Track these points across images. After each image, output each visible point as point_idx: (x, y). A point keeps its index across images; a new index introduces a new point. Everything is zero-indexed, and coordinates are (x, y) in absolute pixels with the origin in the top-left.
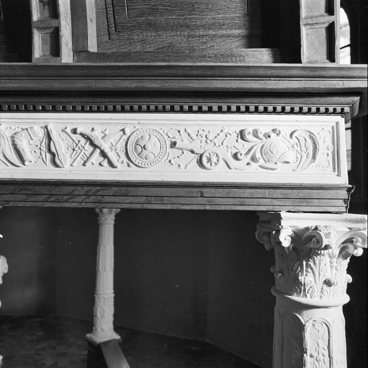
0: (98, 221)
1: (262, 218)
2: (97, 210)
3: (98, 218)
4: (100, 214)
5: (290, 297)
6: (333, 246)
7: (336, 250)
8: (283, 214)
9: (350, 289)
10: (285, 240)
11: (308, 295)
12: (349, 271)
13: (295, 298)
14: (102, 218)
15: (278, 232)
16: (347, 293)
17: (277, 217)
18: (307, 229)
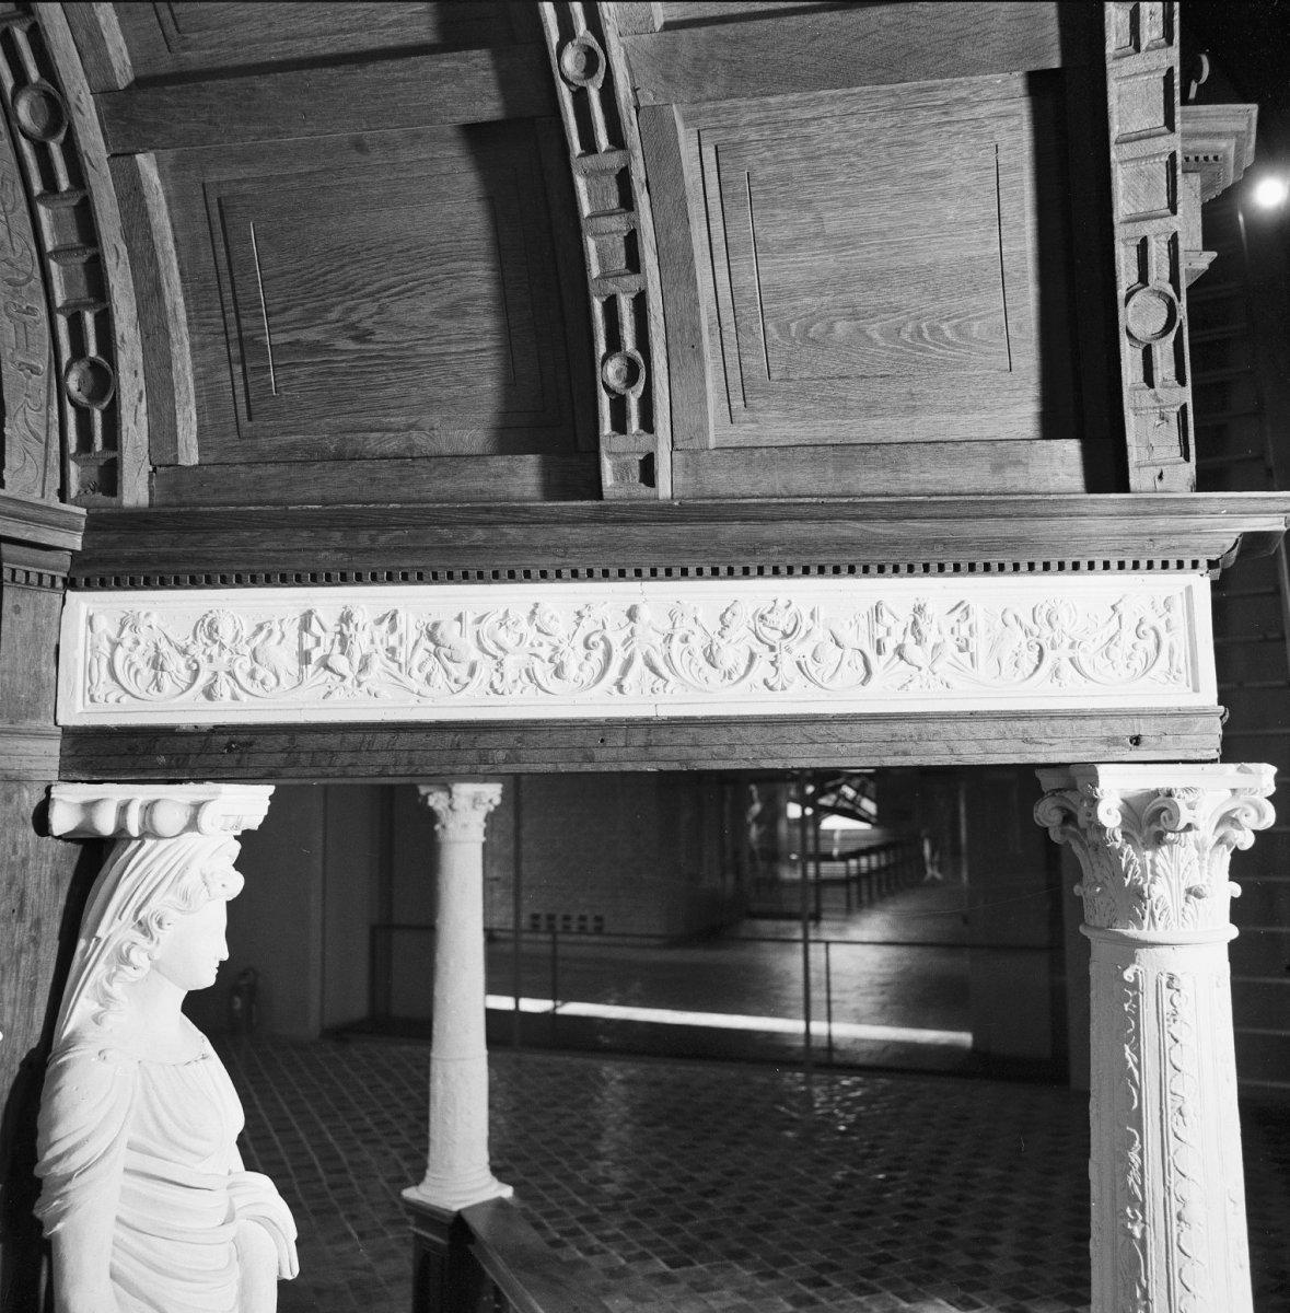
0: (435, 834)
1: (1048, 781)
2: (437, 801)
3: (437, 827)
4: (445, 815)
5: (1121, 930)
6: (1201, 824)
7: (1207, 832)
8: (1101, 769)
9: (1238, 911)
10: (1109, 815)
11: (1160, 924)
12: (1235, 873)
13: (1132, 932)
14: (451, 826)
15: (1094, 802)
16: (1232, 921)
17: (1088, 771)
18: (1156, 793)
